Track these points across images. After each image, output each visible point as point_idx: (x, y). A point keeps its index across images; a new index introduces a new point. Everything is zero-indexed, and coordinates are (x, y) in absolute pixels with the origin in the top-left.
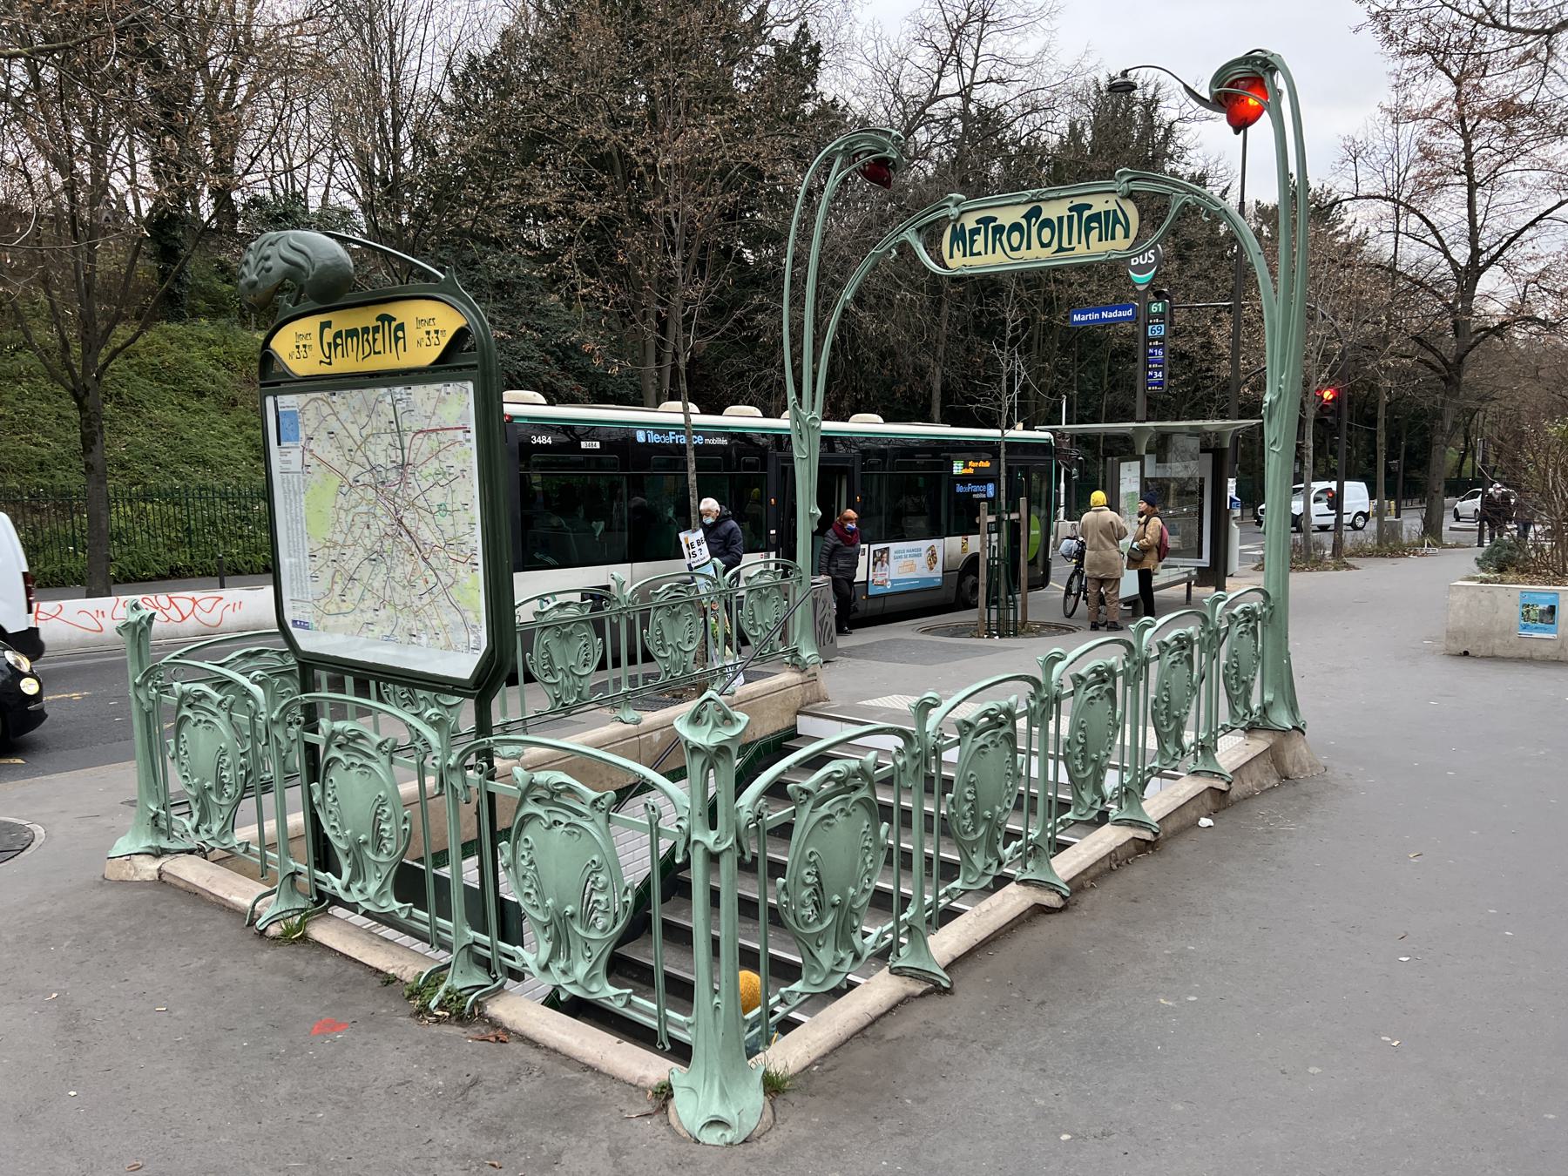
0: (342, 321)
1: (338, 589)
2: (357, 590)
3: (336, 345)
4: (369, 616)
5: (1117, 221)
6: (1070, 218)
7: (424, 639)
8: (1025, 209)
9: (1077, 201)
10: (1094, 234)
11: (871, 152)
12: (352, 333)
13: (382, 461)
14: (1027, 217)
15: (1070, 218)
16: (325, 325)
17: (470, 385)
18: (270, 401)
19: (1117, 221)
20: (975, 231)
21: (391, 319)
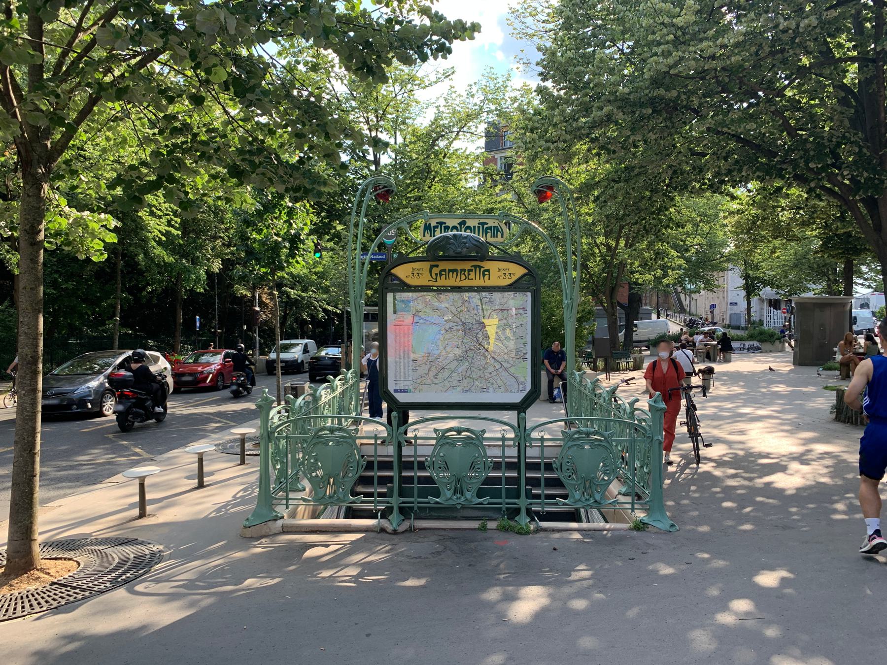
0: (443, 265)
1: (432, 374)
2: (446, 374)
3: (441, 275)
4: (455, 383)
5: (498, 231)
6: (479, 227)
7: (491, 389)
8: (460, 220)
9: (482, 221)
10: (489, 235)
11: (385, 187)
12: (453, 271)
13: (471, 321)
14: (460, 224)
15: (479, 227)
16: (432, 267)
17: (529, 294)
18: (390, 297)
19: (498, 231)
20: (435, 227)
21: (480, 267)
